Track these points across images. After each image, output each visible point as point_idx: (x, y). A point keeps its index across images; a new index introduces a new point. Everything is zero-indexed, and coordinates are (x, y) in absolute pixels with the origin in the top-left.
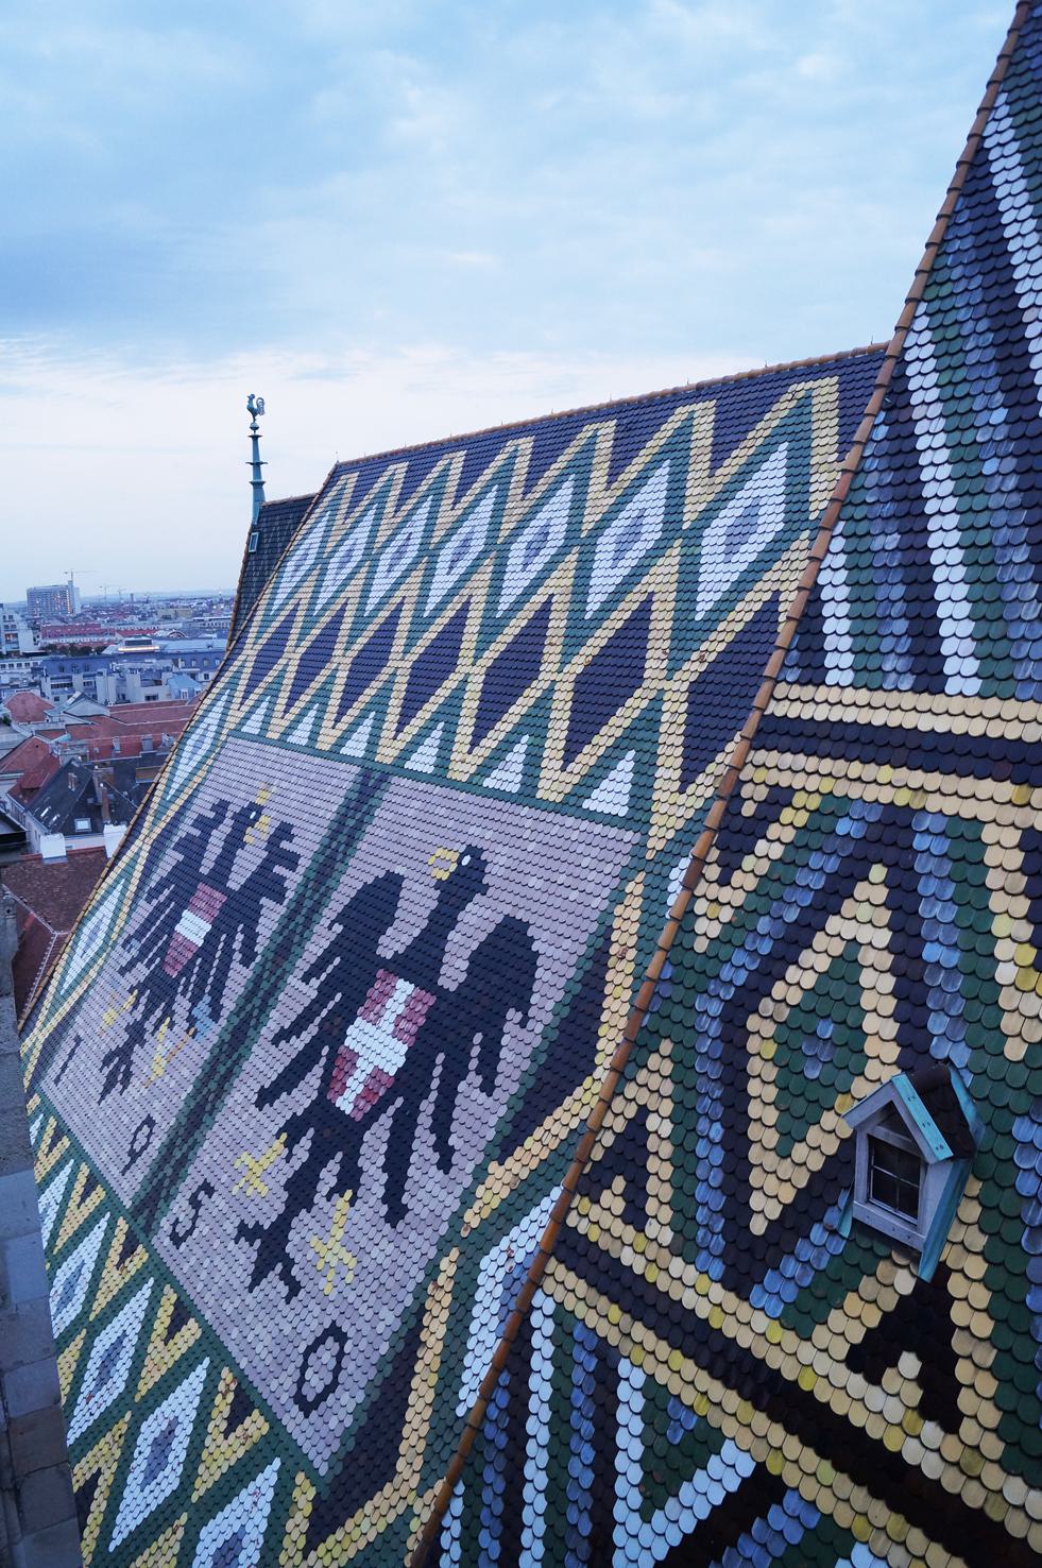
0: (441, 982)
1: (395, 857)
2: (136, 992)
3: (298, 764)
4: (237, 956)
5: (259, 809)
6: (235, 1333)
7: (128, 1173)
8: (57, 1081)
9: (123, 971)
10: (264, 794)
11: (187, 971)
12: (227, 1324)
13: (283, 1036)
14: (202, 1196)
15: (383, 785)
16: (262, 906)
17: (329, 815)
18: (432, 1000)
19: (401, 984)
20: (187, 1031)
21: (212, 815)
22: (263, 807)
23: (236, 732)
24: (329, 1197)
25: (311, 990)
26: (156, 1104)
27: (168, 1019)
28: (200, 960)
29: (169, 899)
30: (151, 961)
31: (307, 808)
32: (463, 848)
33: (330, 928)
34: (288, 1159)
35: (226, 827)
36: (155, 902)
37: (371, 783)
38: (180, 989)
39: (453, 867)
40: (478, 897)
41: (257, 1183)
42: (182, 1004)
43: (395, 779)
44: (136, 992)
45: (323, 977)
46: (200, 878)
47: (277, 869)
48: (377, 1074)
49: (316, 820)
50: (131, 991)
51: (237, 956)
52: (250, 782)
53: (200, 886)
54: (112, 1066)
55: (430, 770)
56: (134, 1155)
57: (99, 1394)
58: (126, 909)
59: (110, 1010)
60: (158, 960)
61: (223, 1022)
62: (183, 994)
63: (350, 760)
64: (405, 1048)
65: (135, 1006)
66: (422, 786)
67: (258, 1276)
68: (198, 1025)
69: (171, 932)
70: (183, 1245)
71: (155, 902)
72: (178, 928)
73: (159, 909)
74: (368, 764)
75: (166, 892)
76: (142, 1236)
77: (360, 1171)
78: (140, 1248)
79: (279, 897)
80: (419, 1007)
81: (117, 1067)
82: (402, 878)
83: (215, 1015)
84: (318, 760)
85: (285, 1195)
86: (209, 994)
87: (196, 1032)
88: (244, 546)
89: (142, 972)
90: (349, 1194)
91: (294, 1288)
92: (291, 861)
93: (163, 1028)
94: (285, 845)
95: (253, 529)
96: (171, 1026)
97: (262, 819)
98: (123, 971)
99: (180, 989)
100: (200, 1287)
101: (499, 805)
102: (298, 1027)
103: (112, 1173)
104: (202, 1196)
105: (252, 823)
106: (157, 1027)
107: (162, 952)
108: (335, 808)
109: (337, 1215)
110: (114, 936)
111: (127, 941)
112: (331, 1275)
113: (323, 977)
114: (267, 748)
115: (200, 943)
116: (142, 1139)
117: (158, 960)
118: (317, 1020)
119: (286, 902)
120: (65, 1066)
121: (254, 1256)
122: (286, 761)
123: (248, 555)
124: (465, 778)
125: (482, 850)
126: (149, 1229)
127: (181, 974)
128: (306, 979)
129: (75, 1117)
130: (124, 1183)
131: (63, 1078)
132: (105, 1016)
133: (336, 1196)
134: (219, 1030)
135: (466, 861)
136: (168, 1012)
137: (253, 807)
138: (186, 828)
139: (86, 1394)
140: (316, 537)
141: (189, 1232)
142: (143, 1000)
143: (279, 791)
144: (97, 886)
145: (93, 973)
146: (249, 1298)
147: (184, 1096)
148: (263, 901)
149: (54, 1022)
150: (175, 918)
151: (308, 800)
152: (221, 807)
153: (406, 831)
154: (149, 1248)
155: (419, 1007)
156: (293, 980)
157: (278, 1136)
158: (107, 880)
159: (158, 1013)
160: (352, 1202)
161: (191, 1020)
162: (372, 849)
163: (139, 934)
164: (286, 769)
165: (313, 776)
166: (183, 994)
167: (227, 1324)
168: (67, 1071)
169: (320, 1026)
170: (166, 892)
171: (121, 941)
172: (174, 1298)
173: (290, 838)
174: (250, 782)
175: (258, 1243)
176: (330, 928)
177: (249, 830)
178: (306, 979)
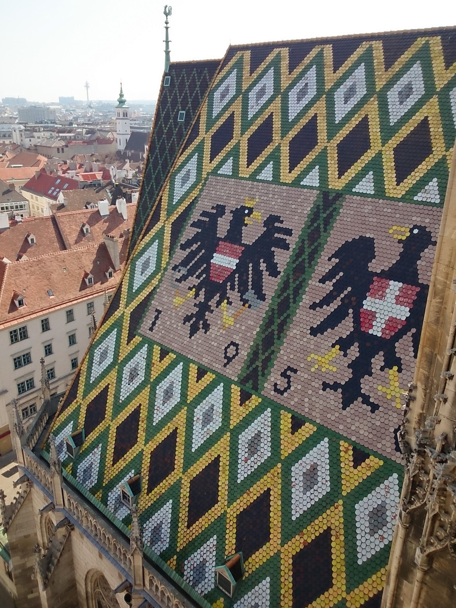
0: (420, 281)
1: (364, 230)
2: (194, 290)
3: (271, 189)
4: (266, 274)
5: (251, 210)
6: (341, 427)
7: (228, 366)
8: (151, 329)
9: (179, 281)
10: (252, 202)
11: (231, 278)
12: (337, 425)
13: (313, 306)
14: (289, 373)
15: (340, 199)
16: (274, 252)
17: (305, 212)
18: (418, 289)
19: (391, 282)
20: (244, 305)
21: (215, 211)
22: (253, 208)
23: (214, 172)
24: (382, 369)
25: (329, 286)
26: (235, 336)
27: (226, 301)
28: (237, 275)
29: (199, 249)
30: (198, 277)
31: (287, 209)
32: (411, 226)
33: (330, 259)
34: (345, 355)
35: (228, 217)
36: (188, 250)
37: (330, 198)
38: (228, 288)
39: (408, 234)
40: (430, 246)
41: (327, 366)
42: (234, 295)
43: (347, 196)
44: (194, 290)
45: (334, 281)
46: (220, 239)
47: (276, 235)
48: (391, 320)
49: (296, 214)
50: (190, 289)
51: (266, 274)
52: (237, 197)
53: (220, 243)
54: (191, 322)
55: (373, 192)
56: (229, 360)
57: (252, 459)
58: (166, 253)
59: (177, 298)
60: (204, 276)
61: (269, 300)
62: (232, 288)
63: (311, 188)
64: (408, 309)
65: (197, 295)
66: (370, 199)
67: (346, 404)
68: (249, 303)
69: (209, 264)
70: (285, 394)
71: (188, 250)
72: (212, 261)
73: (192, 255)
74: (324, 190)
75: (194, 247)
76: (253, 392)
77: (400, 359)
78: (254, 396)
79: (286, 247)
80: (410, 292)
81: (196, 323)
82: (373, 239)
83: (262, 297)
84: (285, 187)
85: (351, 370)
86: (252, 289)
87: (250, 307)
88: (160, 83)
89: (194, 281)
90: (396, 368)
91: (375, 408)
92: (289, 232)
93: (224, 304)
94: (276, 225)
95: (166, 74)
96: (229, 303)
97: (254, 213)
98: (179, 281)
99: (228, 288)
100: (307, 410)
101: (430, 208)
102: (327, 300)
103: (218, 367)
104: (289, 373)
105: (249, 215)
106: (219, 303)
107: (207, 271)
108: (309, 209)
109: (391, 377)
110: (164, 265)
111: (174, 268)
112: (398, 400)
113: (334, 281)
114: (243, 181)
115: (234, 268)
116: (231, 351)
117: (204, 276)
118: (339, 299)
119: (291, 250)
120: (154, 324)
121: (341, 396)
122: (260, 188)
123: (163, 89)
124: (400, 196)
125: (425, 227)
126: (256, 388)
127: (225, 282)
128: (322, 281)
129: (173, 344)
130: (228, 371)
131: (156, 328)
132: (174, 300)
133: (386, 369)
134: (268, 304)
135: (416, 231)
136: (223, 297)
137: (243, 208)
138: (195, 216)
139: (243, 458)
140: (232, 80)
141: (289, 387)
142: (202, 293)
143: (260, 201)
144: (138, 242)
145: (155, 282)
146: (344, 412)
147: (255, 333)
148: (273, 249)
149: (134, 304)
150: (208, 258)
151: (285, 204)
152: (221, 210)
153: (367, 219)
154: (260, 396)
155: (410, 292)
156: (313, 283)
157: (333, 346)
158: (143, 240)
159: (217, 298)
160: (400, 371)
161: (245, 302)
162: (342, 226)
163: (184, 263)
164: (263, 191)
165: (285, 194)
166: (232, 288)
167: (337, 425)
168: (157, 325)
169: (342, 300)
170: (194, 247)
171: (170, 268)
172: (290, 415)
173: (282, 222)
174: (237, 197)
175: (340, 390)
176: (330, 259)
177: (246, 218)
178: (322, 281)
